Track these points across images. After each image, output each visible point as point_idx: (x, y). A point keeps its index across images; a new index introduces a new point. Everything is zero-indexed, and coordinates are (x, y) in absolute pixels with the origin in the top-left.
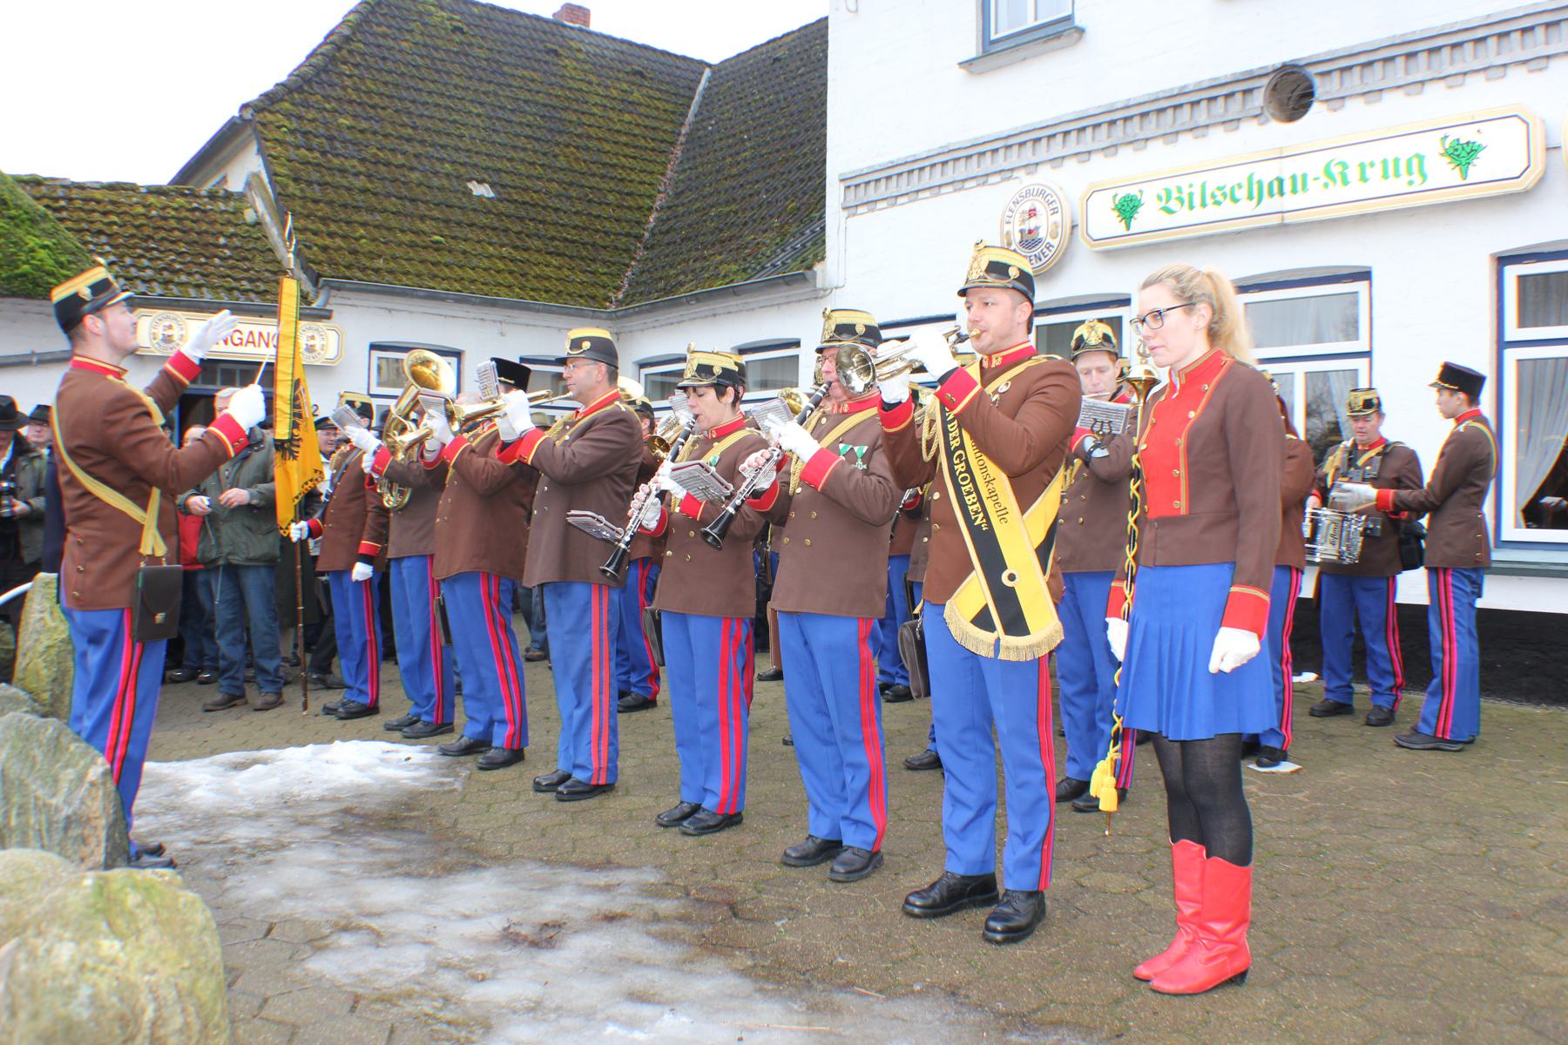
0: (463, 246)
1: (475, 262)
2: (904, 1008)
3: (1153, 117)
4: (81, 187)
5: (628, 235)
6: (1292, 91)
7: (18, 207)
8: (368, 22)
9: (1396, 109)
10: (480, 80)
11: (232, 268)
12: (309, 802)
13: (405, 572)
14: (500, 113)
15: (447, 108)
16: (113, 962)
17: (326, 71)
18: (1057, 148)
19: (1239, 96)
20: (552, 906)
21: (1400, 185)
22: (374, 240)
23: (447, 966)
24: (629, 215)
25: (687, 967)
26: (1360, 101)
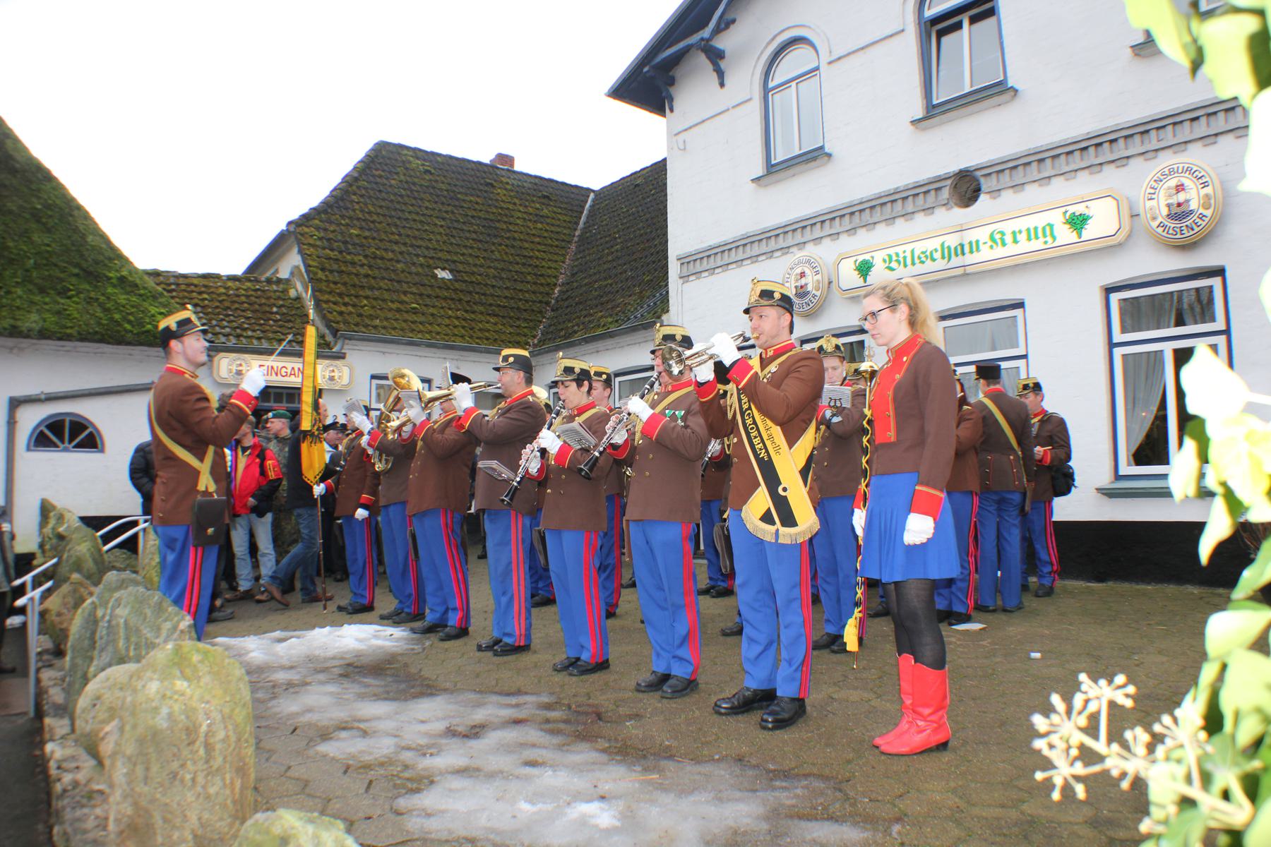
0: (431, 310)
1: (440, 320)
2: (707, 768)
3: (878, 209)
4: (185, 276)
5: (541, 302)
6: (966, 187)
7: (145, 288)
8: (370, 168)
9: (1033, 193)
10: (443, 204)
11: (281, 327)
12: (326, 659)
13: (391, 514)
14: (456, 225)
15: (421, 222)
16: (182, 695)
17: (342, 199)
18: (818, 232)
19: (933, 193)
20: (479, 715)
21: (1037, 244)
22: (373, 307)
23: (409, 748)
24: (542, 289)
25: (565, 748)
26: (1011, 191)
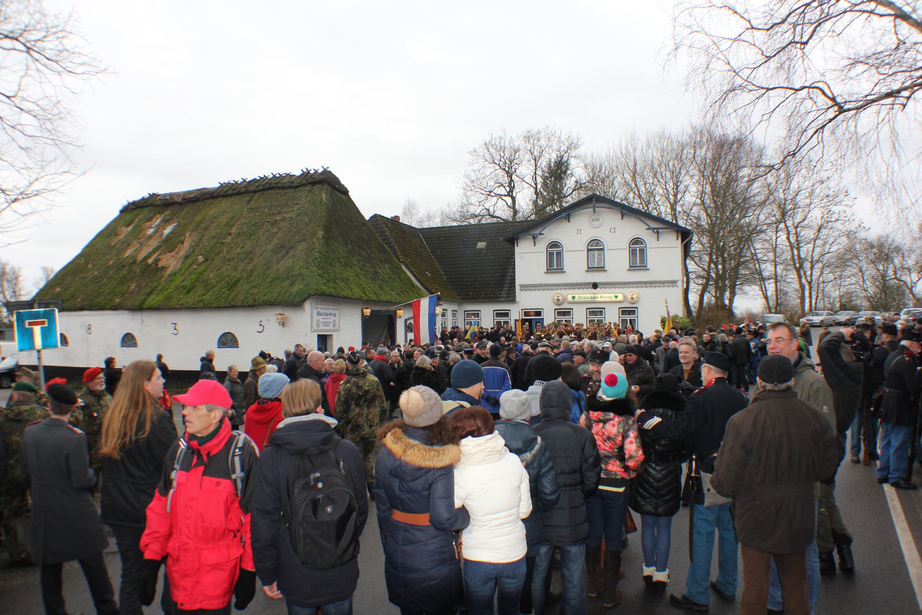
6: (595, 286)
